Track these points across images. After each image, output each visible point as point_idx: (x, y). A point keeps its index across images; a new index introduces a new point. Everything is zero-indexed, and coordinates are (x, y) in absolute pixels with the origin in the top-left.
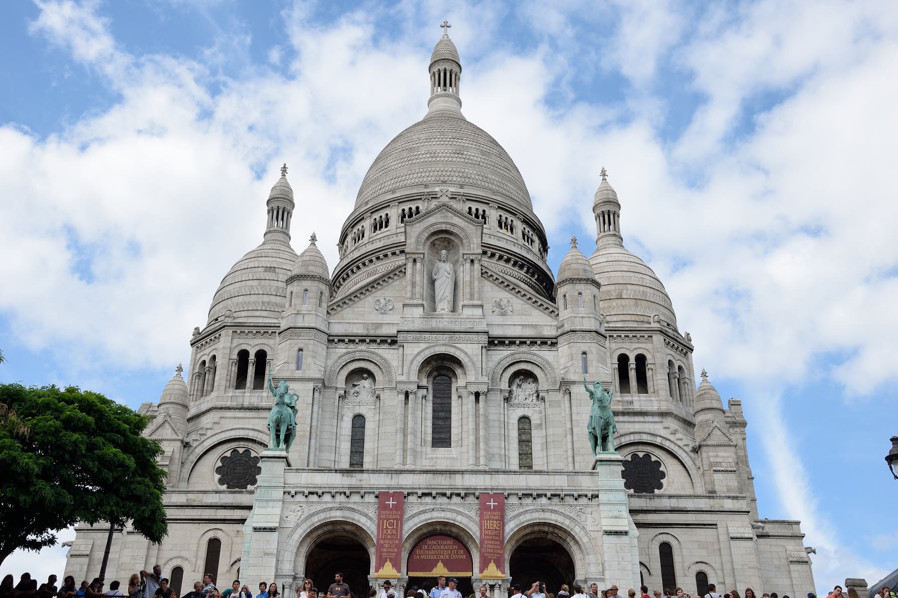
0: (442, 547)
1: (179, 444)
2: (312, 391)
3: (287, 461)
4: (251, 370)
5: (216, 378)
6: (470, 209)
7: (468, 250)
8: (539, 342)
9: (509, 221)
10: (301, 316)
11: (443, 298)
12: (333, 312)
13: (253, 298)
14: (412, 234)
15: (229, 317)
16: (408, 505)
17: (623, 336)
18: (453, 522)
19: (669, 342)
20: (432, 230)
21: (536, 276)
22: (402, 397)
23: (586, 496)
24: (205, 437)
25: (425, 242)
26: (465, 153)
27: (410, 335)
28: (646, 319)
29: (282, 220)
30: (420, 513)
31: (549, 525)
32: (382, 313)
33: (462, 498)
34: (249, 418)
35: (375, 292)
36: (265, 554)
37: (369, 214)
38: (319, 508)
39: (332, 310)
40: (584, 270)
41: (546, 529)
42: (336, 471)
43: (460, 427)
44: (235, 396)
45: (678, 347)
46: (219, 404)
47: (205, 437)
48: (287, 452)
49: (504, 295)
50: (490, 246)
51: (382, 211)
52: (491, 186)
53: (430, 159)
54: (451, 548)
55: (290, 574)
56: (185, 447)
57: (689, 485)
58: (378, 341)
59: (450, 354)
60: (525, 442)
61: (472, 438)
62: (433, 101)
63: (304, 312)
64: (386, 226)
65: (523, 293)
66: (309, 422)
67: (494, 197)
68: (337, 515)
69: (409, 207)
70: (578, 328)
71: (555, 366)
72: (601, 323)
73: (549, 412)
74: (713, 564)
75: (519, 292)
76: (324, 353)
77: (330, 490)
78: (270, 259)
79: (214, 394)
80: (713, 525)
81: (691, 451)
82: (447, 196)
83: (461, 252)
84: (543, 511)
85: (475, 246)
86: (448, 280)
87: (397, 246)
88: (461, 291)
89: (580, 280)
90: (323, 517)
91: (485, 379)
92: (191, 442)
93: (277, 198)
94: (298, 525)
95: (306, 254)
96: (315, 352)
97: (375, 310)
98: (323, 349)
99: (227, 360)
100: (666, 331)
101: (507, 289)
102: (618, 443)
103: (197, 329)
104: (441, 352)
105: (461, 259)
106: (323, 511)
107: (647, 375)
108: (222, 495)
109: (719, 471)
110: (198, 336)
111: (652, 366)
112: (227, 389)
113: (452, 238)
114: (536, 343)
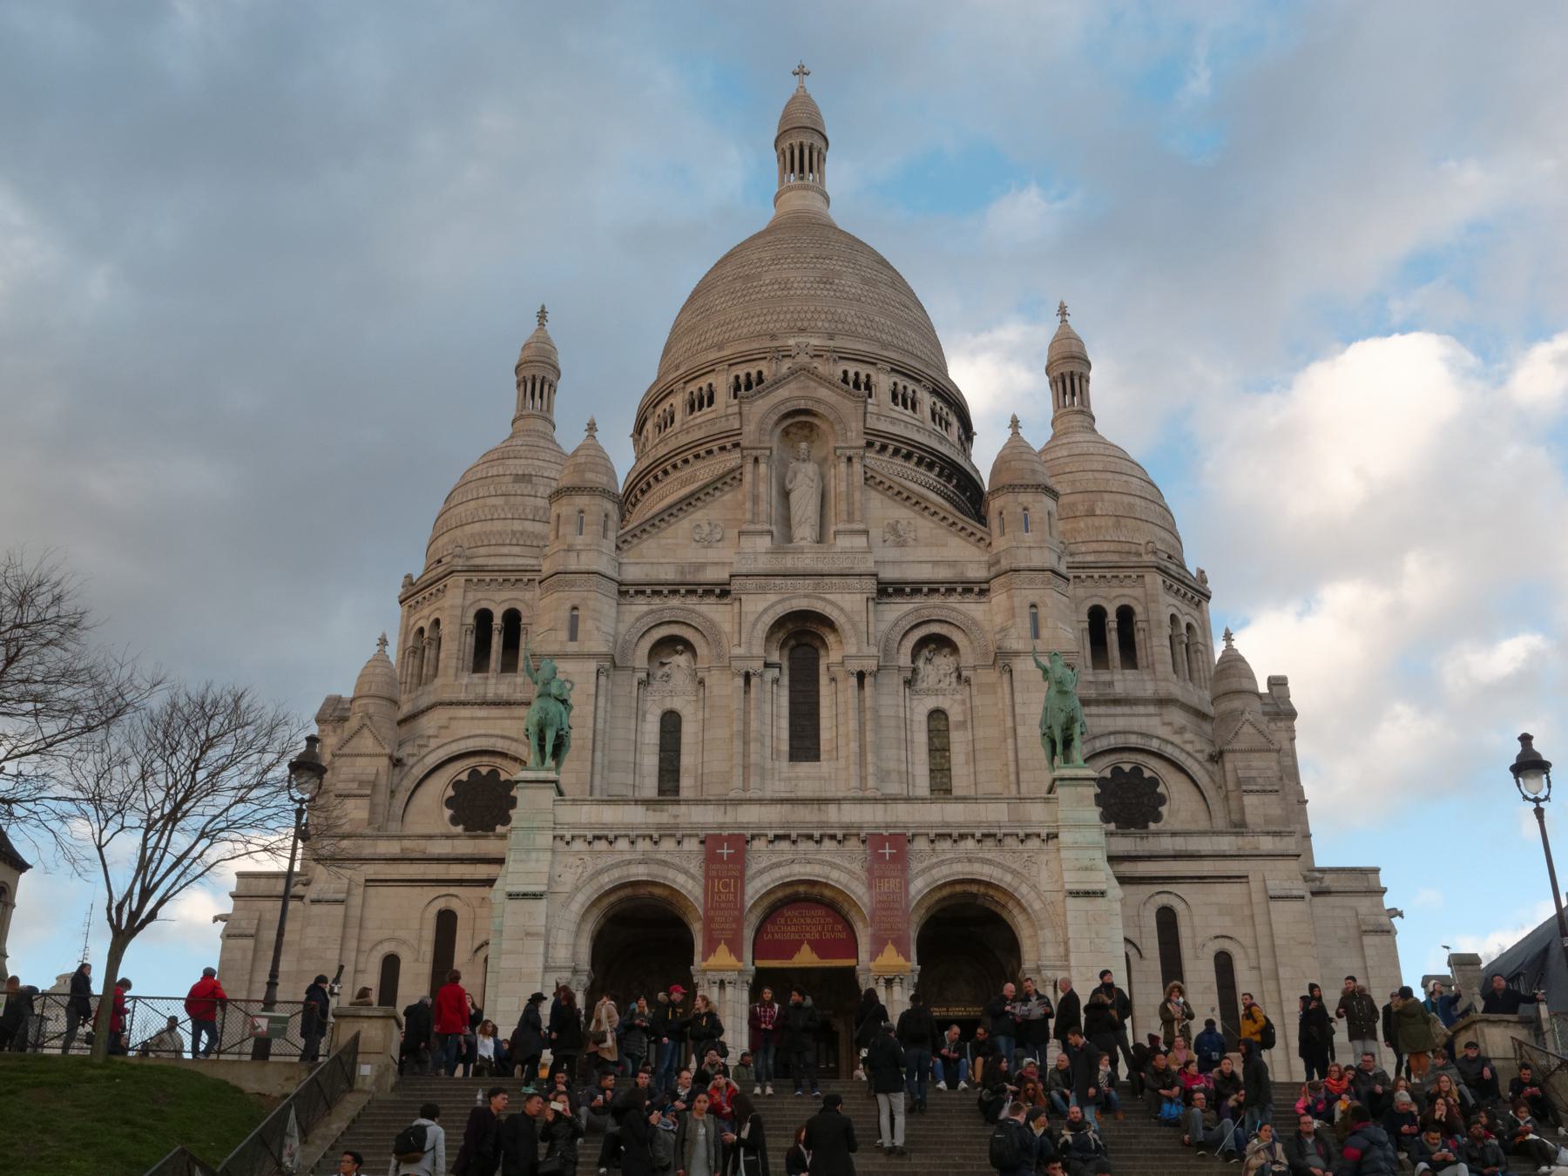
0: (808, 921)
1: (385, 761)
2: (595, 675)
3: (558, 787)
4: (497, 642)
5: (442, 655)
6: (845, 373)
7: (843, 441)
8: (959, 590)
9: (910, 391)
12: (625, 547)
13: (498, 525)
14: (751, 417)
15: (459, 556)
17: (1096, 576)
18: (824, 881)
19: (1171, 586)
20: (784, 409)
21: (955, 481)
22: (740, 681)
24: (425, 751)
25: (772, 431)
28: (1134, 549)
29: (541, 397)
33: (839, 842)
35: (692, 513)
36: (528, 934)
37: (682, 385)
38: (610, 860)
40: (1034, 471)
41: (974, 889)
42: (636, 802)
43: (834, 728)
46: (446, 697)
48: (558, 773)
49: (902, 513)
50: (878, 434)
52: (878, 335)
53: (779, 293)
54: (822, 921)
55: (567, 964)
56: (395, 765)
57: (1203, 815)
60: (939, 749)
61: (854, 746)
62: (783, 197)
63: (579, 548)
64: (711, 402)
66: (591, 725)
67: (885, 353)
68: (640, 872)
69: (746, 371)
70: (1023, 565)
72: (1059, 558)
73: (977, 701)
74: (1241, 940)
75: (926, 508)
76: (614, 615)
78: (523, 461)
79: (438, 682)
80: (1242, 878)
81: (1207, 761)
83: (832, 444)
84: (970, 860)
85: (854, 434)
87: (728, 437)
90: (617, 875)
91: (874, 650)
93: (531, 362)
94: (577, 889)
99: (458, 626)
100: (1166, 567)
101: (907, 503)
103: (409, 577)
105: (831, 457)
106: (617, 865)
107: (1137, 639)
108: (456, 842)
109: (1251, 791)
110: (410, 588)
111: (1144, 625)
112: (459, 672)
113: (816, 421)
114: (955, 590)
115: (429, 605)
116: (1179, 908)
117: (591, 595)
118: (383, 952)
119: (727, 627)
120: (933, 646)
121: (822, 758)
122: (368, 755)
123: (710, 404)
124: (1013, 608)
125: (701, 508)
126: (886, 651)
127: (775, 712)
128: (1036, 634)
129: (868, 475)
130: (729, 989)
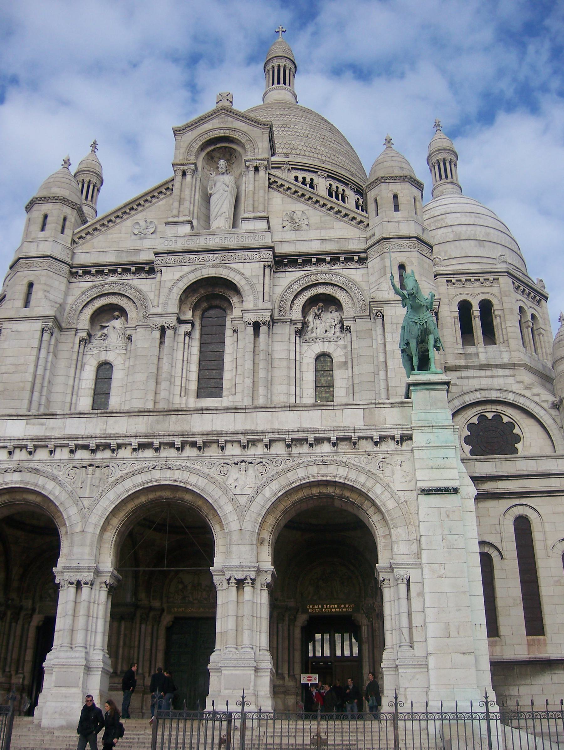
2: (38, 334)
6: (296, 178)
7: (251, 156)
8: (342, 259)
9: (340, 190)
10: (36, 244)
11: (219, 214)
14: (182, 144)
17: (463, 280)
18: (184, 485)
20: (207, 137)
22: (157, 334)
26: (293, 127)
27: (171, 257)
31: (335, 484)
32: (141, 239)
33: (199, 449)
35: (134, 215)
40: (401, 168)
43: (234, 369)
45: (530, 293)
58: (133, 269)
59: (223, 276)
61: (248, 382)
65: (322, 202)
67: (323, 165)
70: (392, 235)
71: (364, 286)
73: (355, 346)
76: (63, 287)
77: (5, 444)
82: (227, 100)
84: (325, 463)
86: (226, 194)
89: (394, 179)
91: (268, 305)
96: (48, 285)
98: (61, 282)
101: (302, 199)
102: (461, 402)
104: (210, 275)
105: (244, 169)
107: (495, 323)
113: (234, 146)
114: (338, 259)
116: (532, 516)
119: (151, 296)
120: (322, 304)
121: (225, 393)
125: (142, 211)
126: (280, 307)
127: (185, 358)
129: (272, 180)
130: (85, 590)
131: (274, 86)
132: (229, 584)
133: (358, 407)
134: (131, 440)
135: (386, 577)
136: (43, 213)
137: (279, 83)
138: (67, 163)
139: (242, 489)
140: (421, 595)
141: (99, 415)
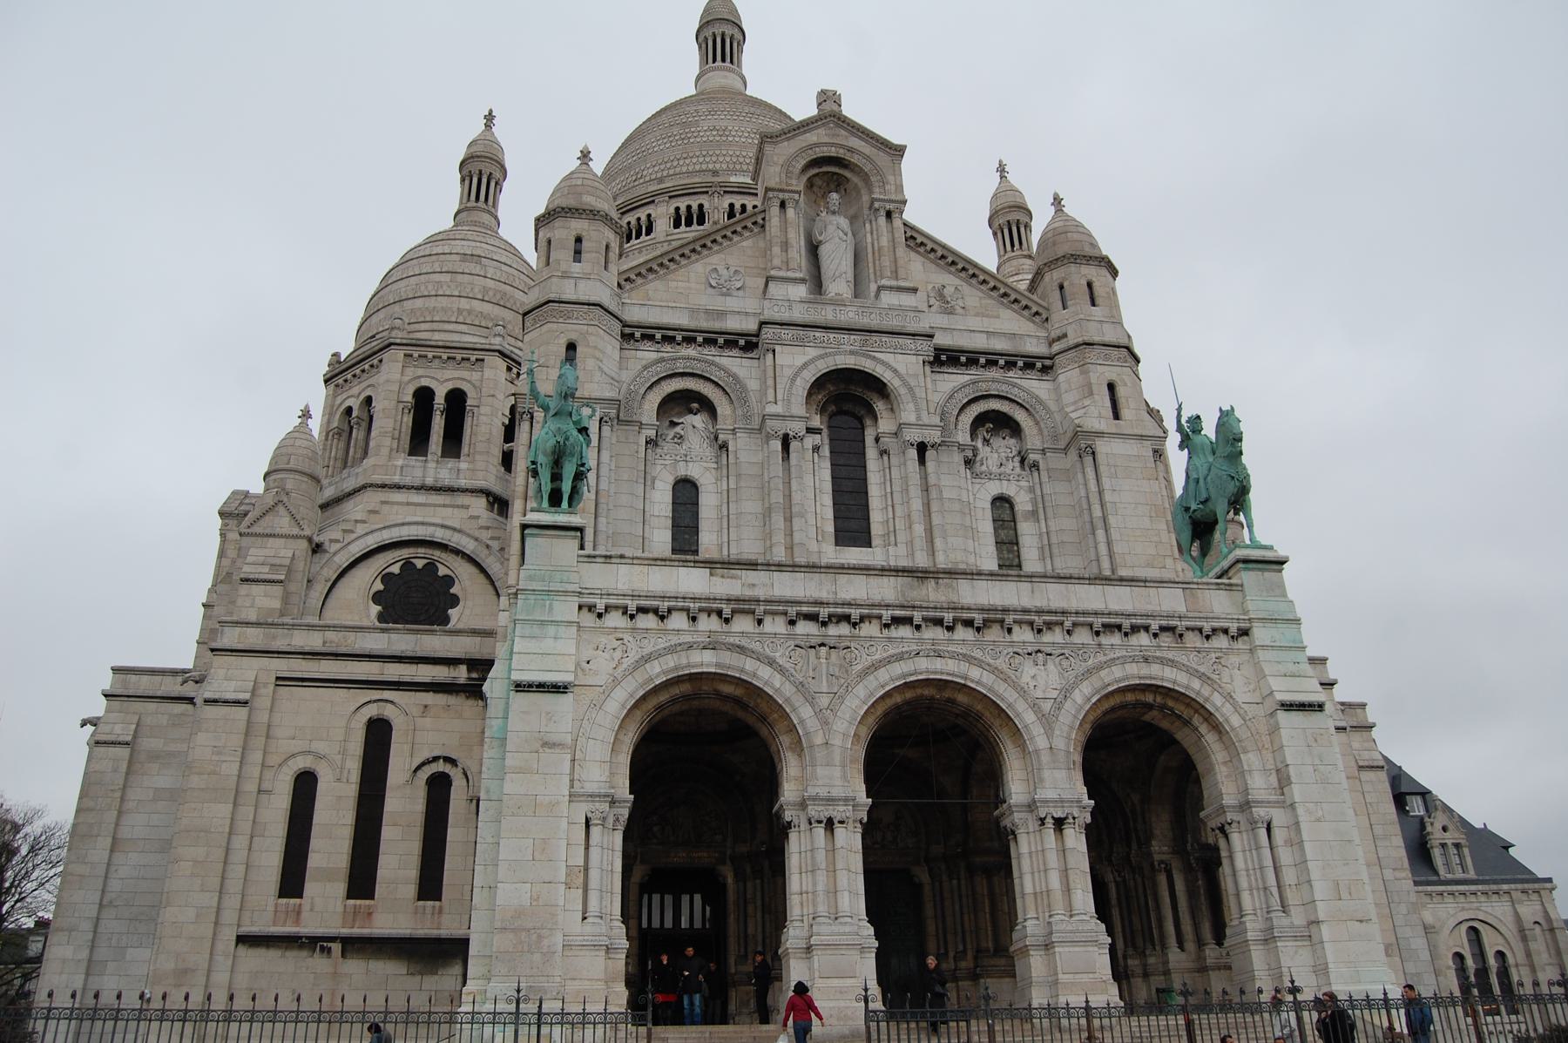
1: (304, 544)
3: (582, 538)
4: (438, 423)
8: (1020, 364)
10: (573, 281)
12: (628, 286)
13: (443, 301)
16: (862, 643)
18: (963, 682)
22: (777, 445)
23: (1226, 631)
24: (354, 536)
27: (787, 332)
30: (889, 661)
32: (723, 295)
33: (978, 630)
34: (435, 505)
36: (545, 744)
38: (662, 643)
39: (626, 280)
40: (1092, 244)
41: (1149, 698)
43: (890, 509)
44: (407, 466)
46: (377, 478)
47: (354, 536)
51: (640, 210)
53: (718, 138)
56: (314, 551)
58: (721, 341)
61: (919, 529)
62: (706, 76)
64: (649, 231)
65: (981, 278)
68: (705, 661)
69: (686, 203)
70: (1097, 339)
71: (1053, 406)
73: (1047, 490)
75: (974, 275)
78: (473, 244)
83: (865, 198)
84: (1146, 660)
88: (871, 265)
90: (672, 664)
92: (327, 543)
93: (478, 157)
94: (616, 682)
95: (575, 176)
97: (707, 286)
99: (394, 403)
101: (952, 269)
105: (866, 211)
106: (671, 650)
115: (360, 382)
117: (591, 329)
118: (296, 768)
119: (753, 385)
122: (282, 536)
123: (648, 234)
124: (1089, 385)
125: (718, 252)
128: (1117, 416)
129: (909, 234)
131: (716, 64)
132: (1043, 824)
133: (1176, 585)
134: (882, 612)
135: (1235, 818)
136: (574, 233)
137: (723, 60)
138: (585, 156)
139: (1044, 692)
140: (1297, 843)
141: (822, 570)
